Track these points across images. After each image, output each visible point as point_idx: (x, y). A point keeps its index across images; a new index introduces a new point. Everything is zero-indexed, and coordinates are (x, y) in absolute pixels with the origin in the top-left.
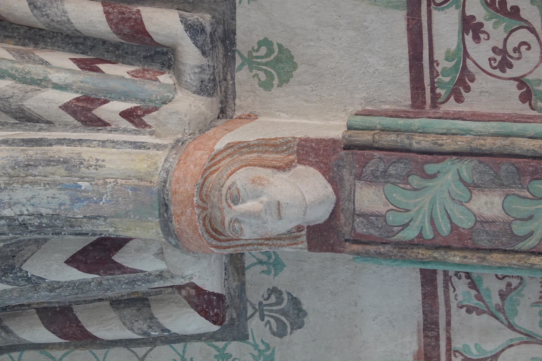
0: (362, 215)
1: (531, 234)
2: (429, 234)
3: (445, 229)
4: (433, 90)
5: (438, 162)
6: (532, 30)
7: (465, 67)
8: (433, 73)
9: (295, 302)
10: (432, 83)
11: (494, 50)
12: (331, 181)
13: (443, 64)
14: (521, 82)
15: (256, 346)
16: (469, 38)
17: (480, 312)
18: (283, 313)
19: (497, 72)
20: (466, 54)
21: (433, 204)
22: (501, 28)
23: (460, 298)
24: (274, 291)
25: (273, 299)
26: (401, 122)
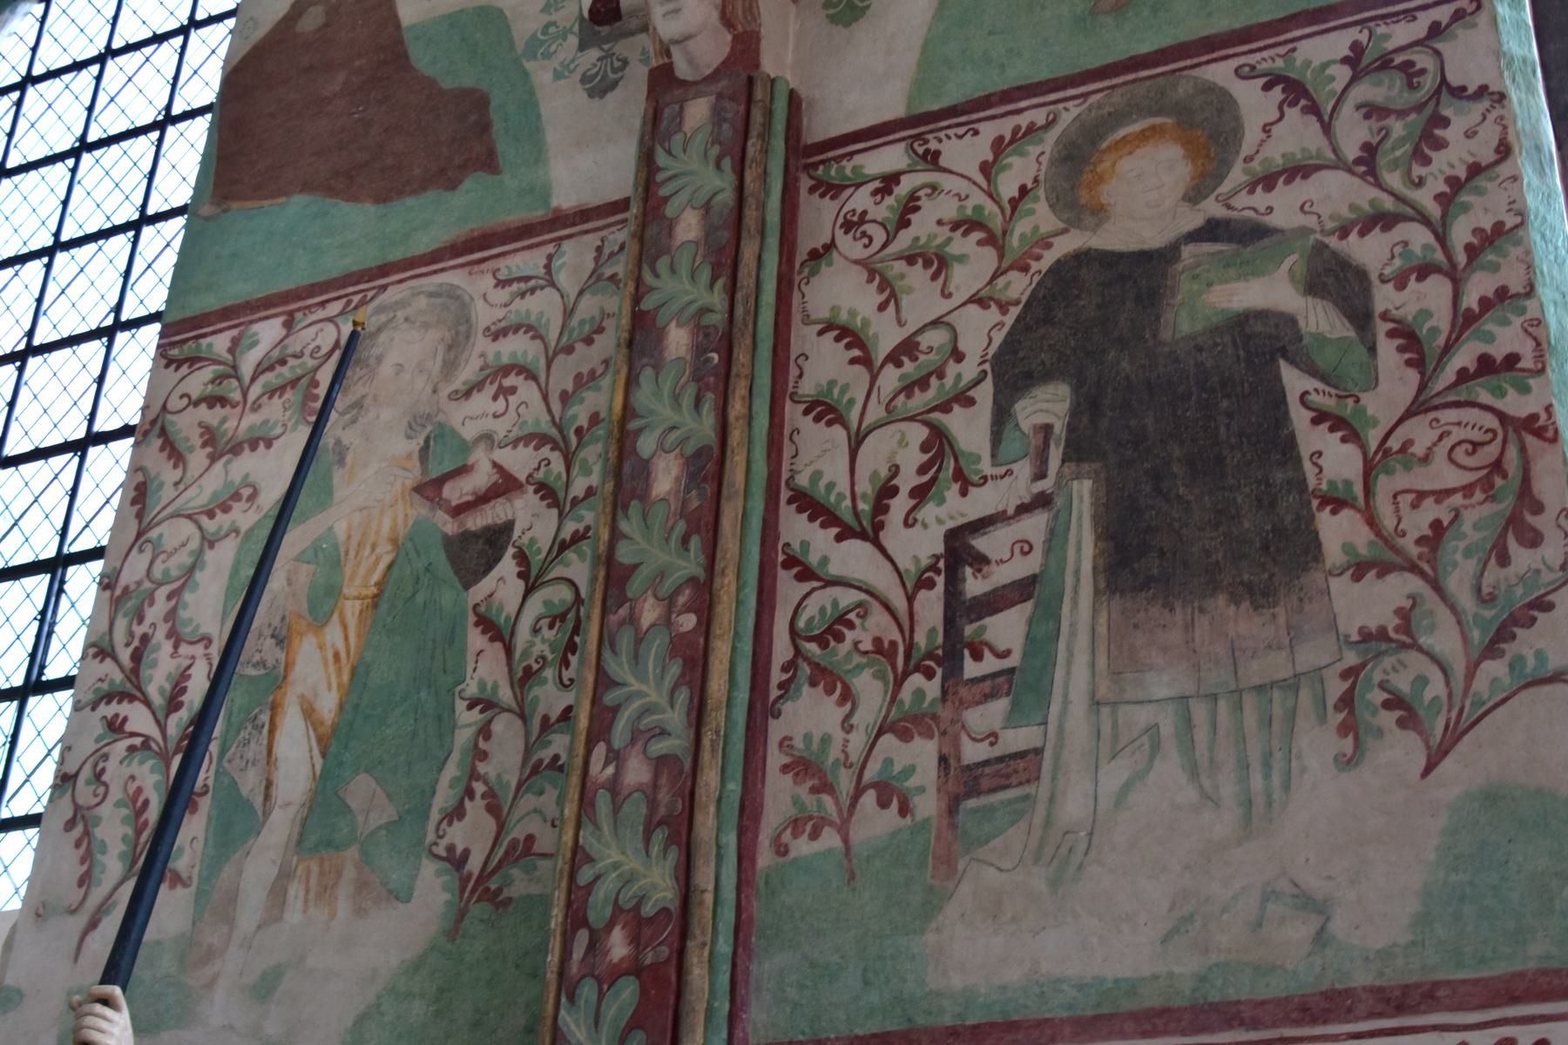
0: (682, 109)
1: (657, 276)
2: (660, 177)
3: (664, 192)
4: (823, 162)
5: (733, 169)
6: (885, 246)
7: (847, 187)
8: (838, 159)
9: (613, 85)
10: (829, 160)
11: (865, 213)
12: (716, 72)
13: (848, 166)
14: (830, 246)
15: (572, 61)
16: (877, 184)
17: (597, 259)
18: (605, 76)
19: (841, 220)
20: (858, 186)
21: (692, 173)
22: (887, 214)
23: (611, 237)
24: (625, 63)
25: (617, 64)
26: (779, 126)
